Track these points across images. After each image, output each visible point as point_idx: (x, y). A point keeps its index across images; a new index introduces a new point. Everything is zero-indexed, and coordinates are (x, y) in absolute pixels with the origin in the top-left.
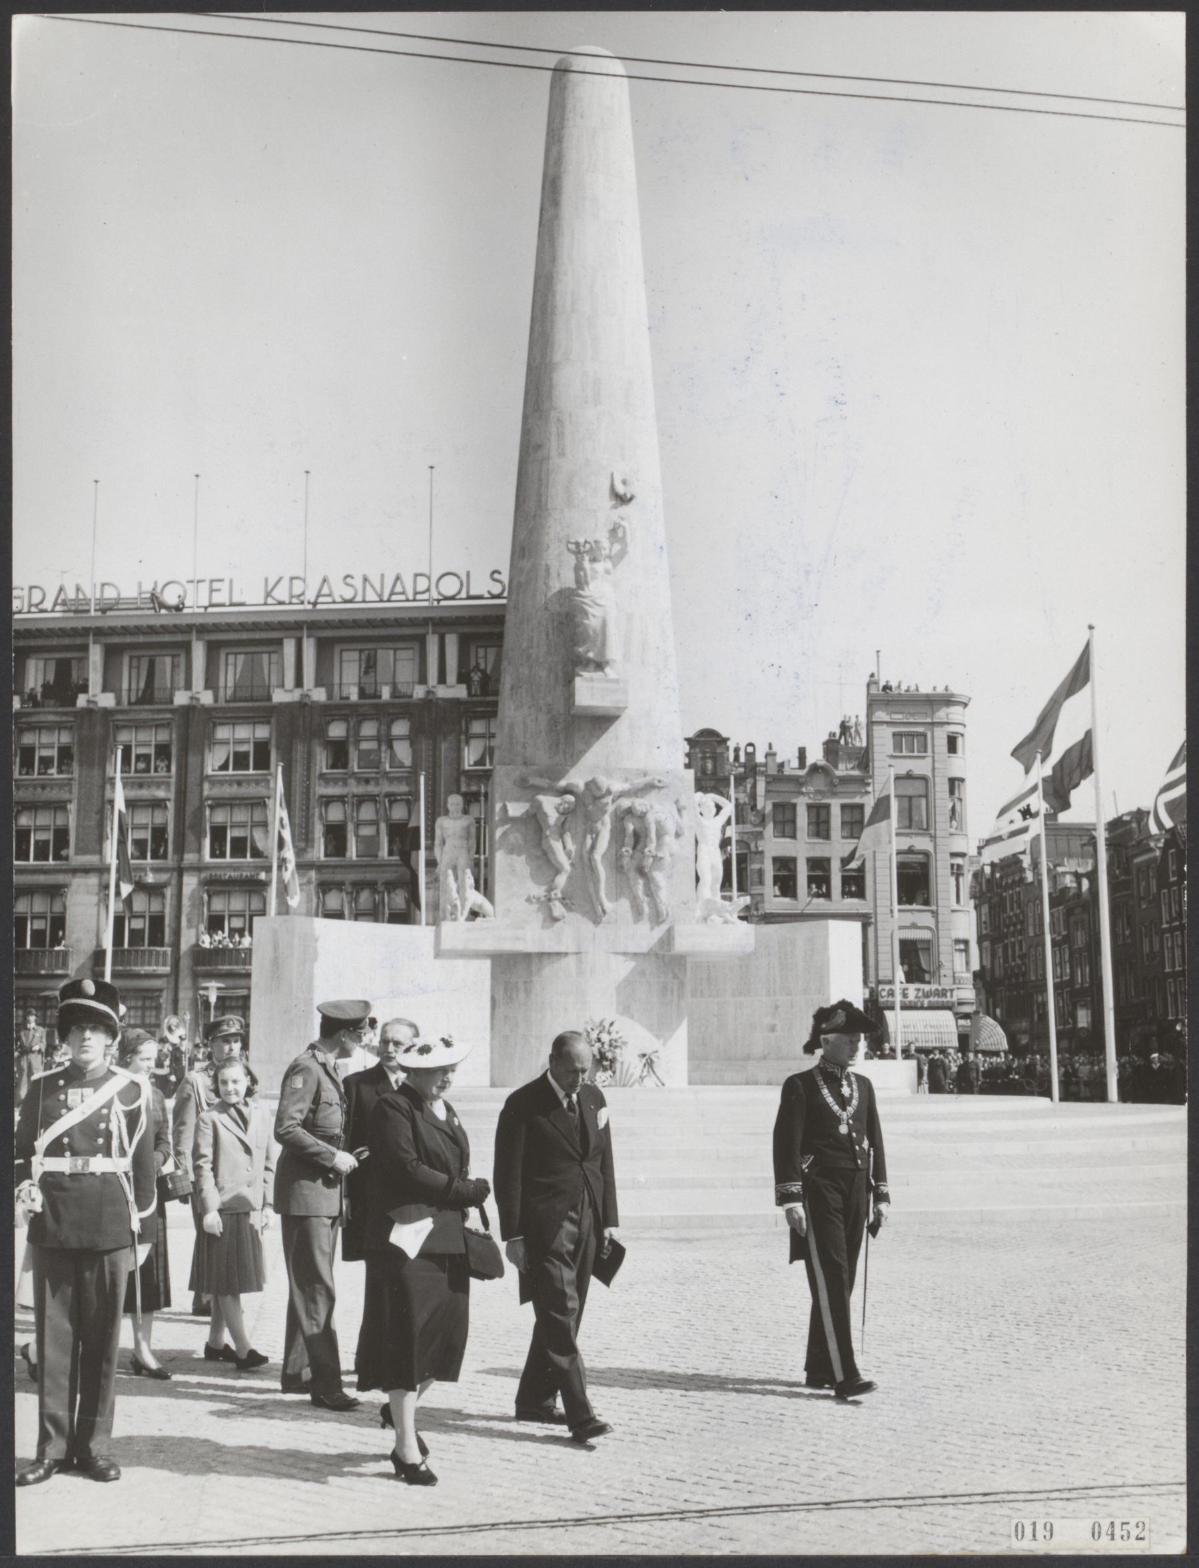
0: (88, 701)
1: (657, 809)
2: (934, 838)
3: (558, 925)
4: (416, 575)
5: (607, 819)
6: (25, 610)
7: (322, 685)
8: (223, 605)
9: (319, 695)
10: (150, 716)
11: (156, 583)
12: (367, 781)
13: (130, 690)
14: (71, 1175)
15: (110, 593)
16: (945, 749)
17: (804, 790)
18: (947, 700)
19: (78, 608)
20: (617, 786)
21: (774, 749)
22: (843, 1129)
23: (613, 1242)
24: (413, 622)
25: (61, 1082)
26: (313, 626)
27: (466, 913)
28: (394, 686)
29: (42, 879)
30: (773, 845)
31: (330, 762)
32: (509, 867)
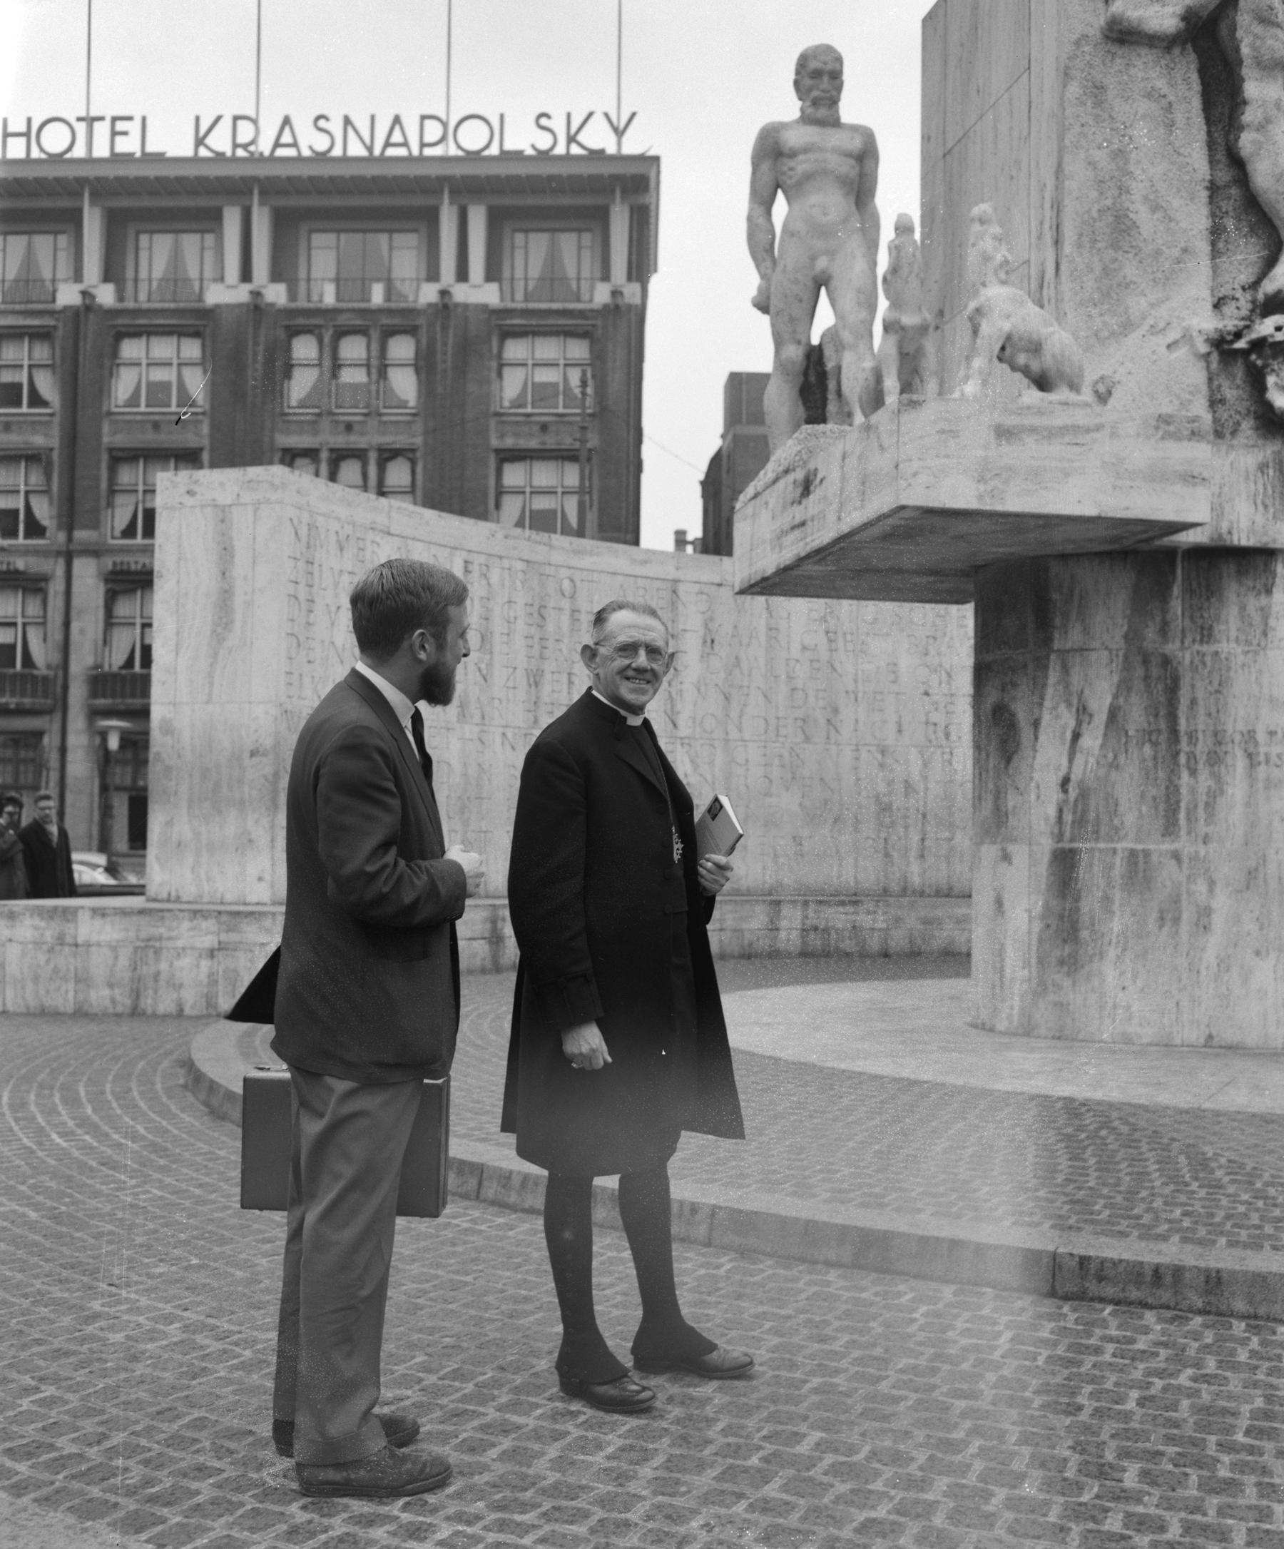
4: (423, 118)
8: (132, 155)
9: (276, 294)
11: (29, 120)
12: (349, 427)
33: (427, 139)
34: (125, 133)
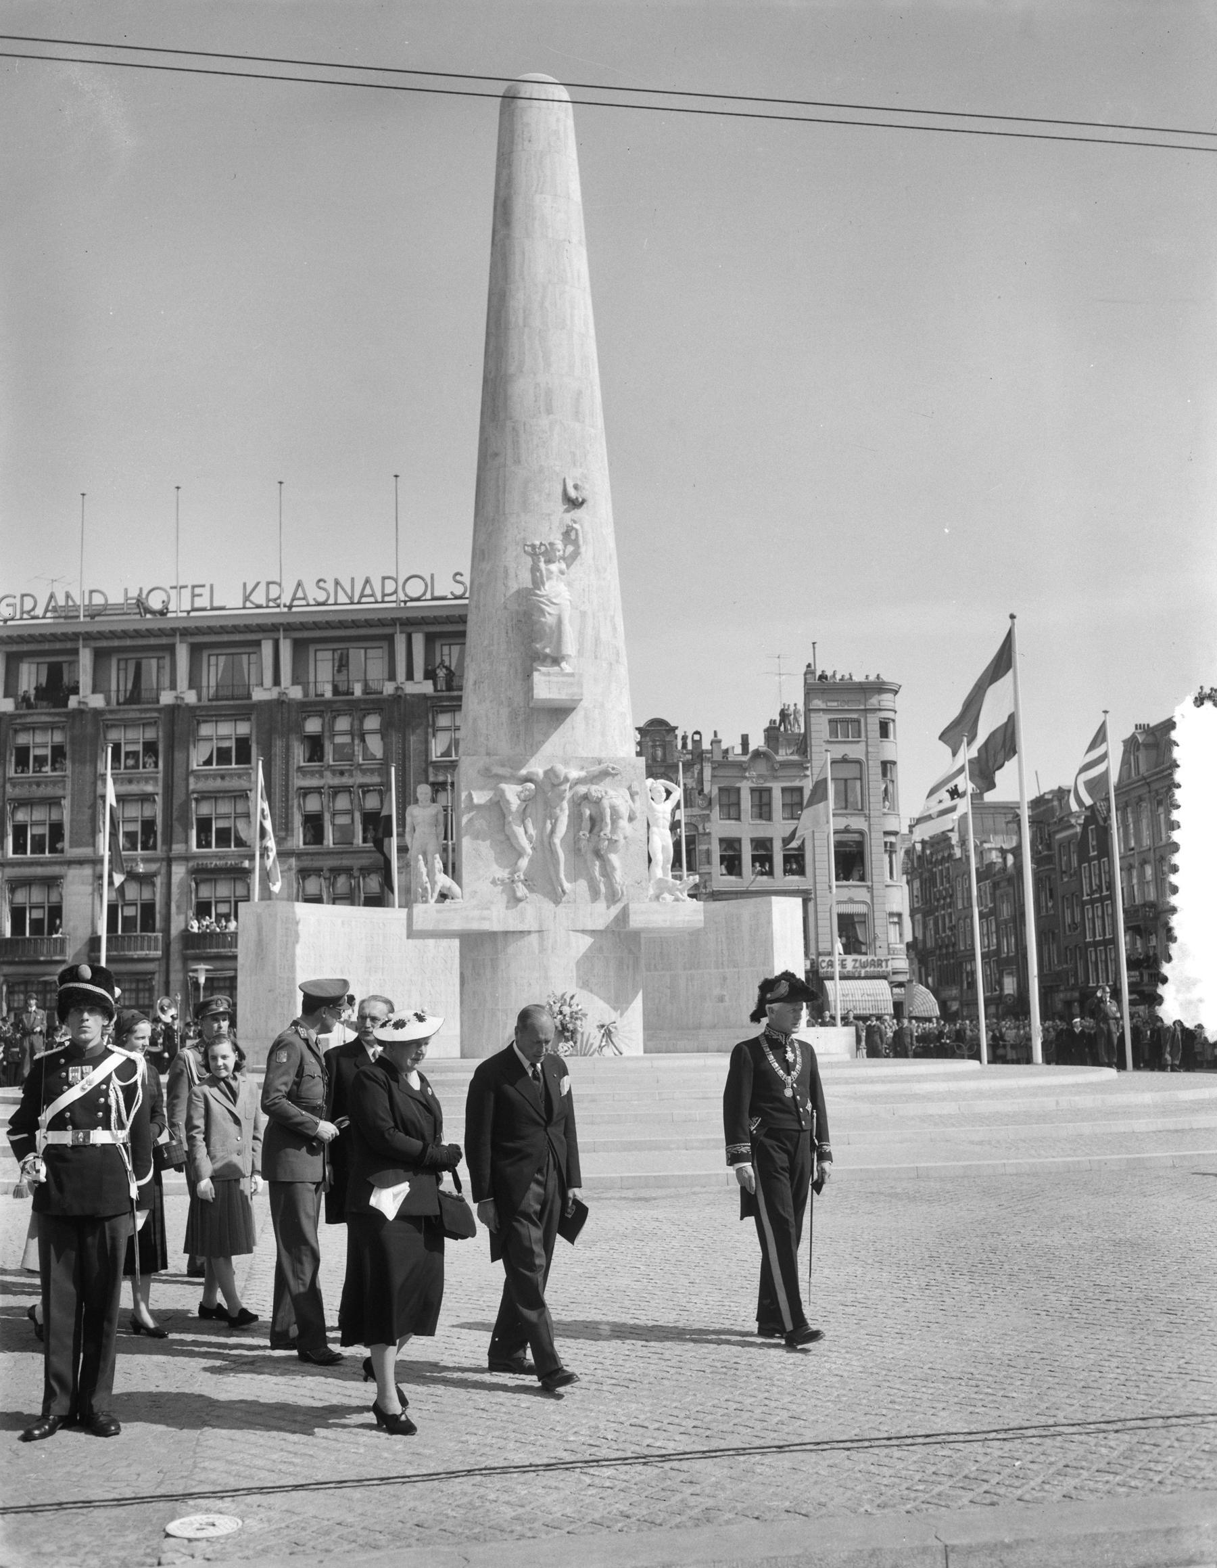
0: (80, 703)
1: (614, 796)
2: (868, 818)
3: (521, 905)
4: (384, 578)
5: (565, 804)
6: (18, 617)
7: (298, 684)
8: (204, 609)
9: (296, 693)
11: (141, 589)
12: (342, 773)
13: (118, 690)
14: (73, 1147)
15: (98, 600)
16: (878, 734)
18: (879, 687)
19: (67, 613)
20: (574, 774)
21: (719, 737)
22: (788, 1093)
23: (577, 1202)
24: (381, 623)
25: (63, 1061)
26: (289, 628)
27: (436, 895)
28: (366, 685)
29: (39, 871)
30: (719, 827)
31: (307, 756)
32: (476, 853)
33: (387, 591)
34: (200, 595)
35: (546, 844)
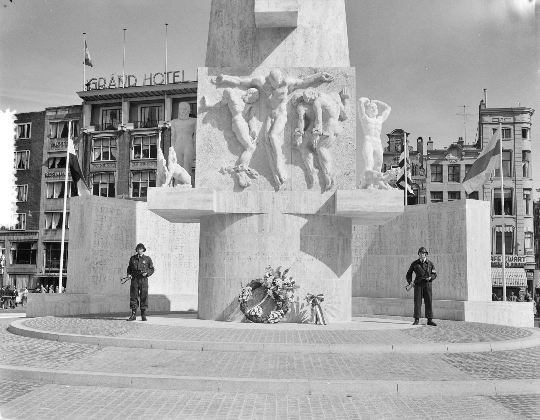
1: (325, 98)
3: (246, 190)
5: (284, 106)
10: (148, 133)
11: (151, 75)
13: (141, 122)
16: (521, 136)
17: (447, 157)
20: (292, 80)
21: (432, 140)
30: (431, 186)
35: (266, 139)
